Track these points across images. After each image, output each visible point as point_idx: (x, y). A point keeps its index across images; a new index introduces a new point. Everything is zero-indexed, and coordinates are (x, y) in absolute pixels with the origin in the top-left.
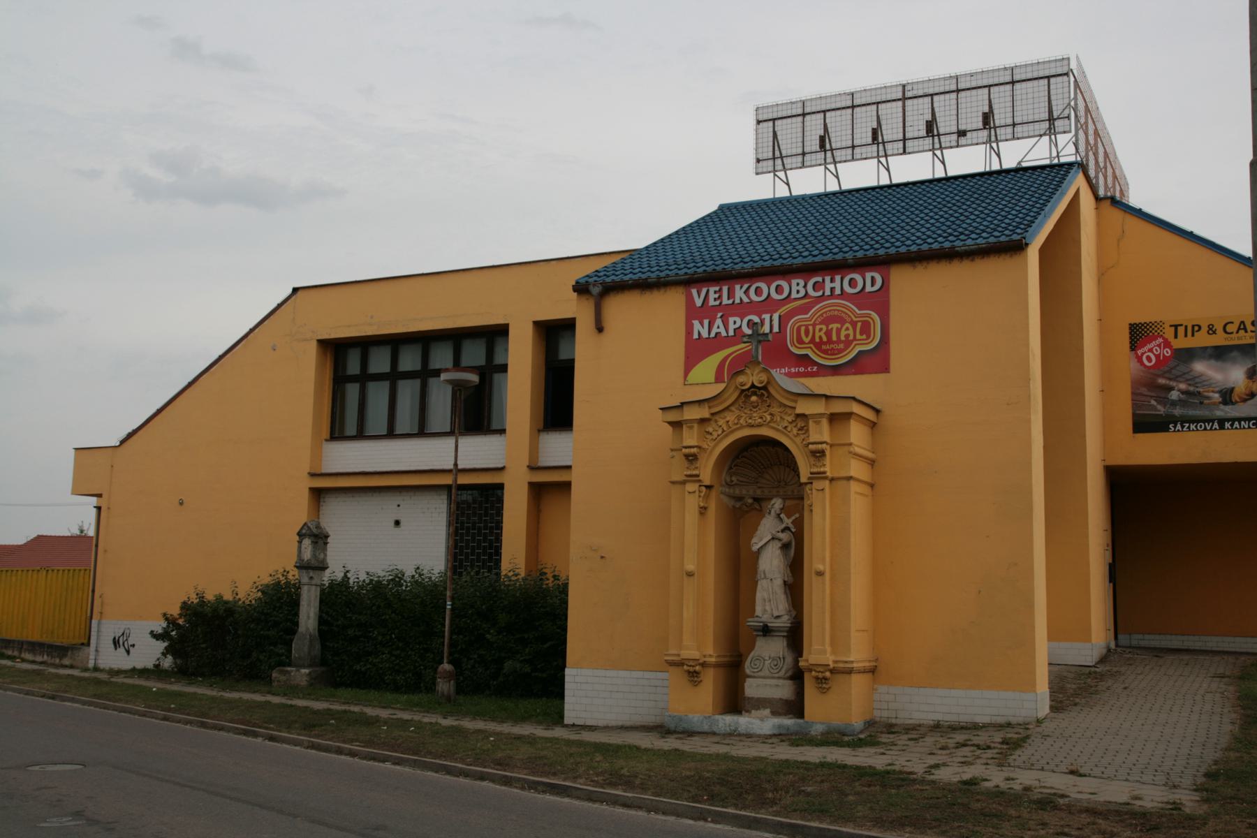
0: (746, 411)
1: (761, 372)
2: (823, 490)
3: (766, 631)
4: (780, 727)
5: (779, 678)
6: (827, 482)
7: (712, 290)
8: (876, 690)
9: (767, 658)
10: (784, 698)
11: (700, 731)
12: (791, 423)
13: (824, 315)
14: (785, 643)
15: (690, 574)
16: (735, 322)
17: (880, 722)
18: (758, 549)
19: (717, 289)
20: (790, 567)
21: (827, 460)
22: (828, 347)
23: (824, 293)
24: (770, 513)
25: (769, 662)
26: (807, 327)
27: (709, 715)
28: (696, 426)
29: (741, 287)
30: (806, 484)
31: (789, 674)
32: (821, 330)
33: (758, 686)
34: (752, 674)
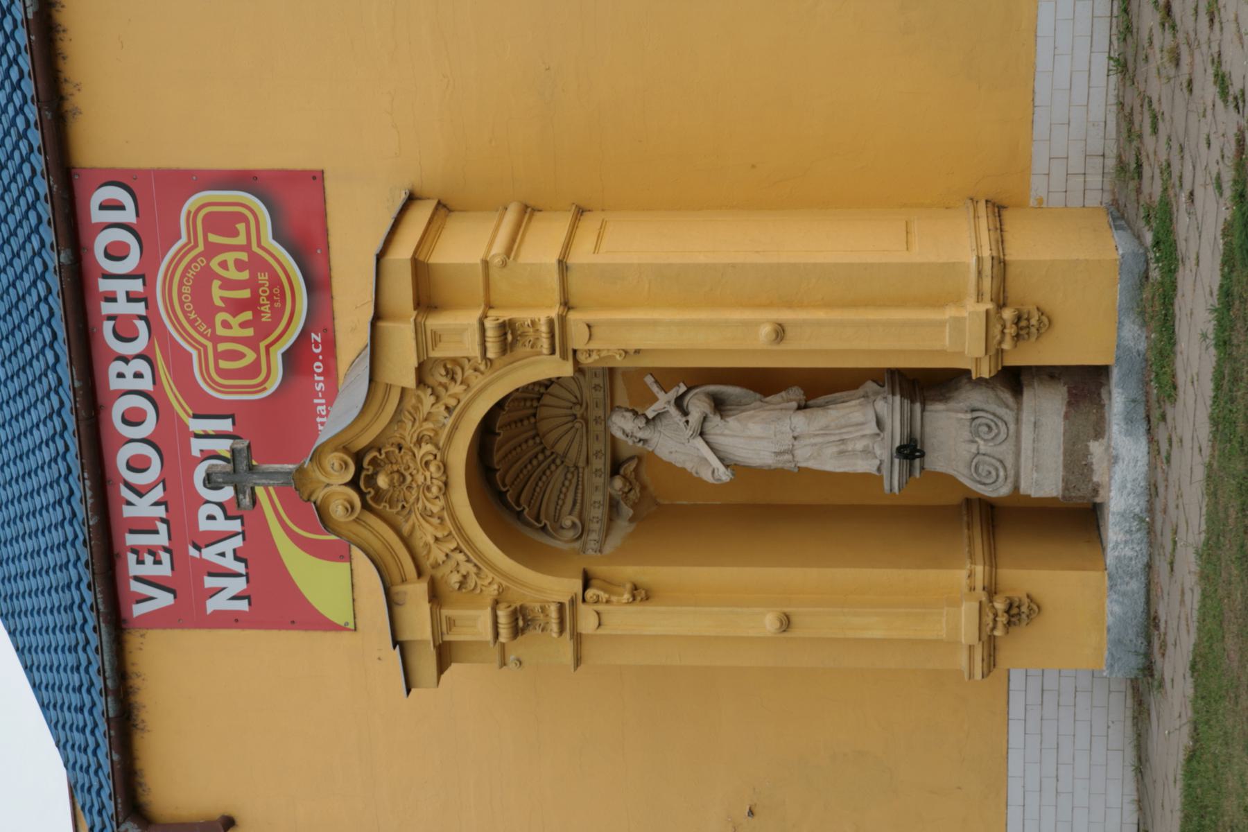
0: (412, 500)
1: (321, 466)
2: (589, 326)
3: (910, 451)
4: (1129, 420)
5: (1018, 421)
6: (573, 316)
7: (134, 569)
8: (1040, 201)
9: (974, 448)
10: (1064, 409)
11: (1143, 600)
12: (438, 399)
13: (193, 316)
14: (939, 406)
15: (786, 623)
16: (211, 517)
17: (1114, 193)
18: (727, 466)
19: (132, 558)
20: (766, 395)
21: (522, 316)
22: (266, 309)
23: (141, 317)
24: (644, 441)
25: (981, 442)
26: (218, 356)
27: (1106, 577)
28: (446, 612)
29: (129, 503)
31: (1007, 396)
32: (226, 324)
33: (1037, 468)
34: (1011, 480)
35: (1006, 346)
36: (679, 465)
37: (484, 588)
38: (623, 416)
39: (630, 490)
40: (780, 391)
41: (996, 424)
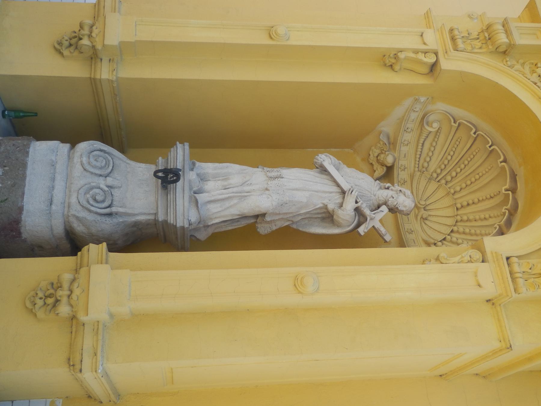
20: (288, 227)
30: (481, 250)
31: (79, 228)
35: (67, 277)
37: (516, 63)
38: (405, 206)
40: (276, 230)
41: (88, 202)
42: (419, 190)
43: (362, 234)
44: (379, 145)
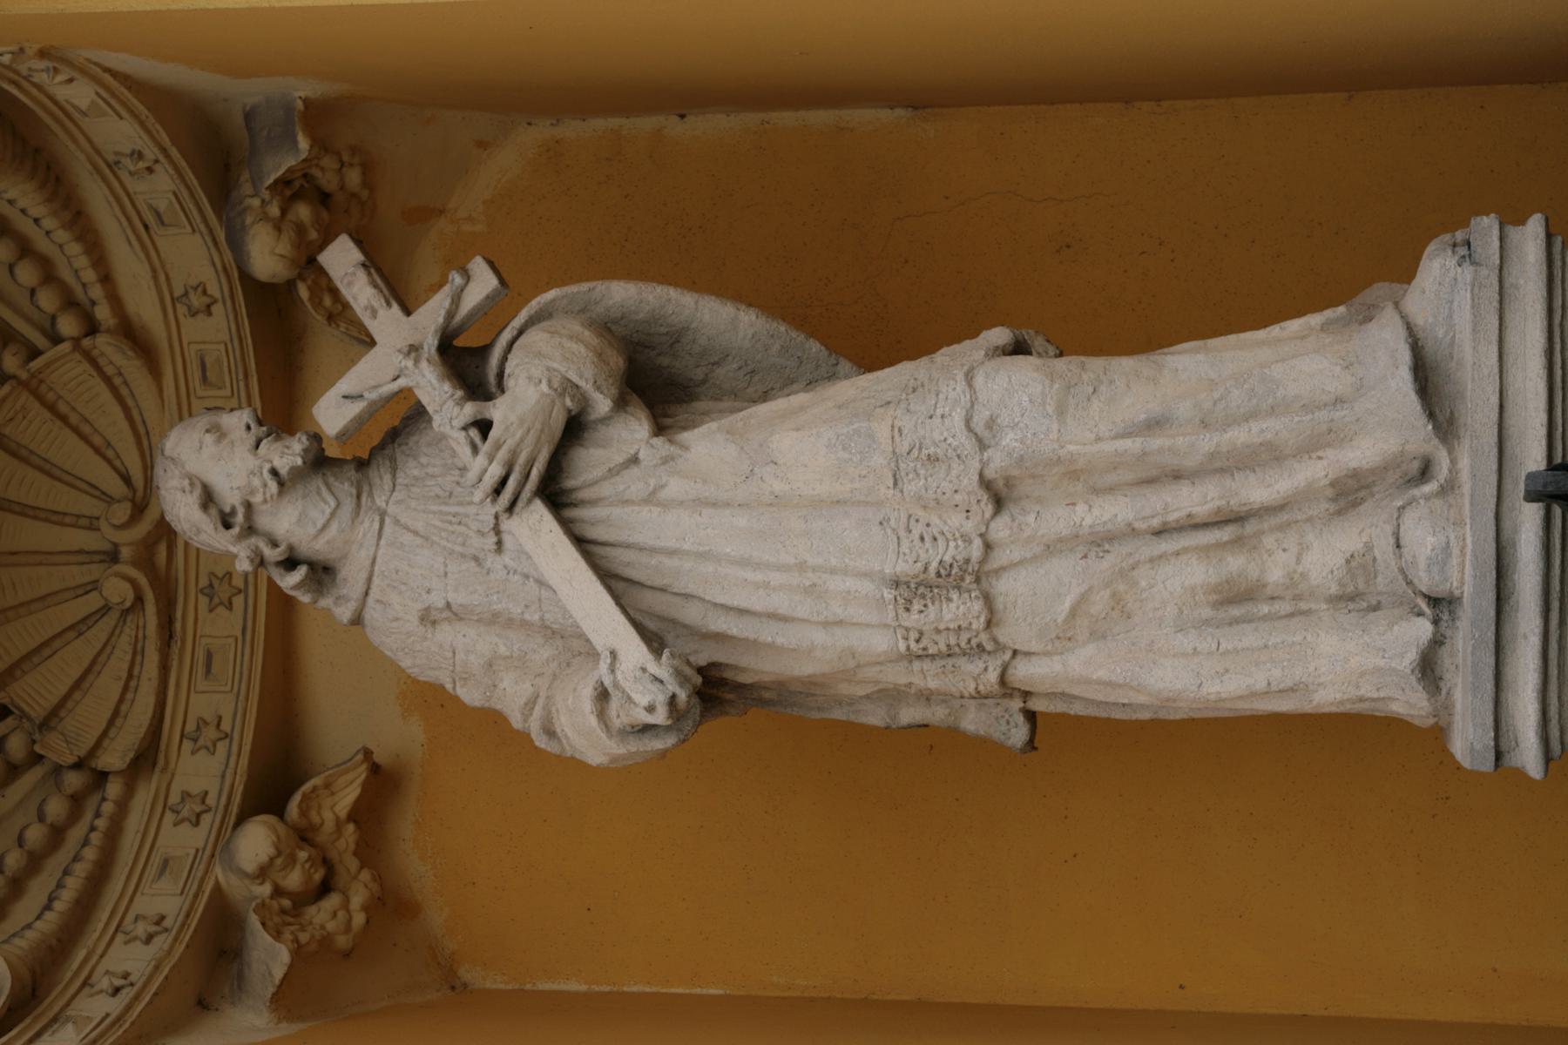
18: (654, 642)
36: (471, 696)
39: (325, 889)
42: (124, 675)
43: (479, 266)
44: (304, 937)
